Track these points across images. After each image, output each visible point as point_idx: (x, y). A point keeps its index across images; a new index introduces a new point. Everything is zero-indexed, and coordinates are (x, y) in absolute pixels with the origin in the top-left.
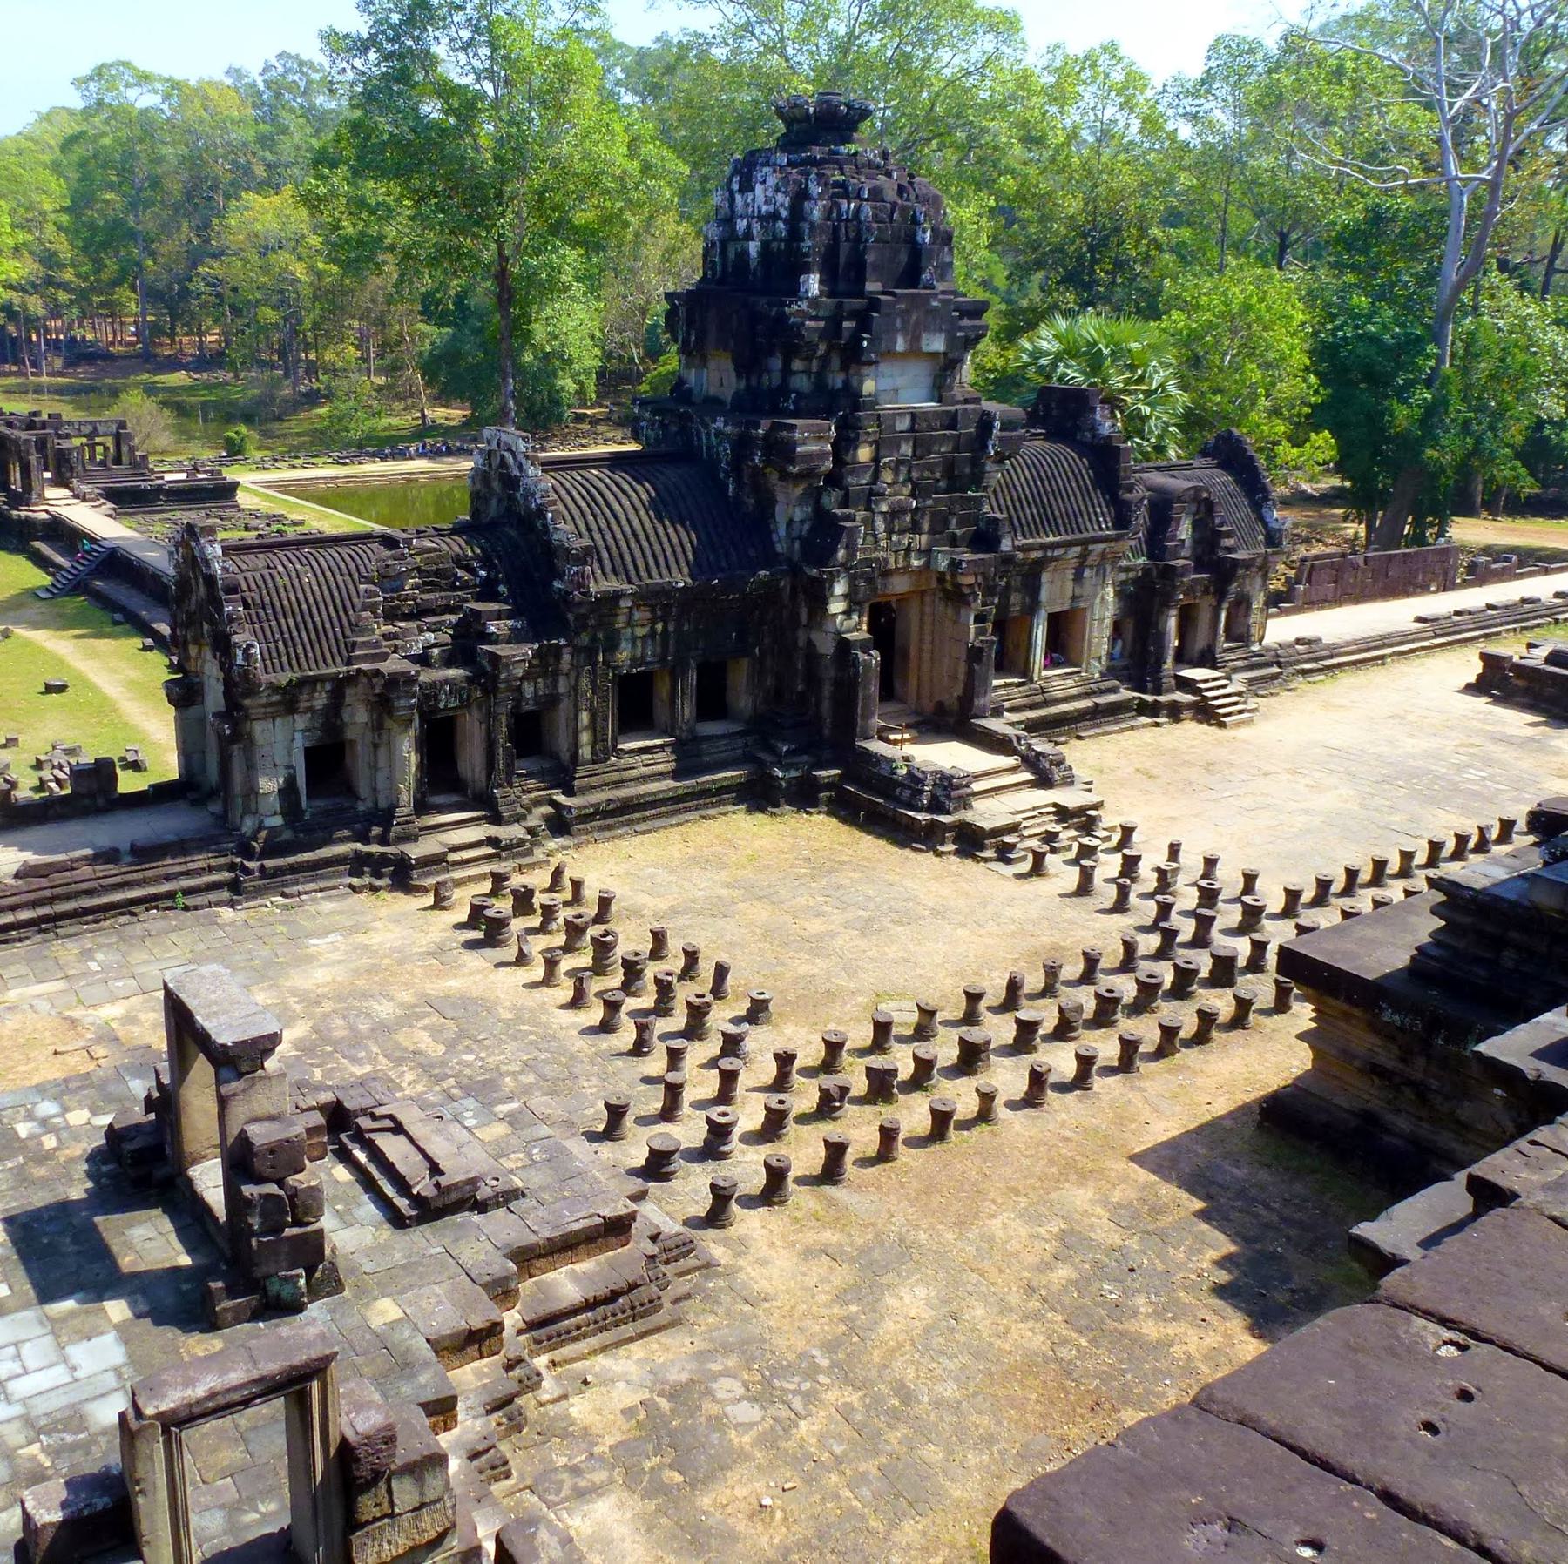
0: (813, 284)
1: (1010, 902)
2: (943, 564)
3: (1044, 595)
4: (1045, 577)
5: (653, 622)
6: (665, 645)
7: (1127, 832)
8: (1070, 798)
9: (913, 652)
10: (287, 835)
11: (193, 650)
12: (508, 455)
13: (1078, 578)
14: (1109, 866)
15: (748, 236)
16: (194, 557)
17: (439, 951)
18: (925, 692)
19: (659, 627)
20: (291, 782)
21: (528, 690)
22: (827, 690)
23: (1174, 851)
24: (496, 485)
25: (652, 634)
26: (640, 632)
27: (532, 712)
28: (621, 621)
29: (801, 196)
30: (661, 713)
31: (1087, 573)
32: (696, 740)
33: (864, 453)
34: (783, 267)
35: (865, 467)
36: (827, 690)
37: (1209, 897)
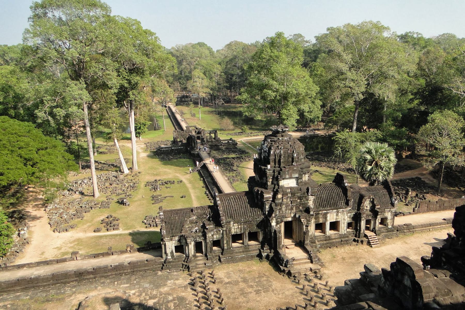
2: (297, 216)
3: (328, 218)
4: (328, 215)
5: (238, 225)
6: (241, 230)
9: (295, 230)
10: (171, 260)
19: (240, 226)
20: (172, 251)
21: (215, 236)
25: (238, 228)
26: (236, 227)
28: (231, 226)
31: (339, 214)
33: (280, 196)
35: (280, 199)
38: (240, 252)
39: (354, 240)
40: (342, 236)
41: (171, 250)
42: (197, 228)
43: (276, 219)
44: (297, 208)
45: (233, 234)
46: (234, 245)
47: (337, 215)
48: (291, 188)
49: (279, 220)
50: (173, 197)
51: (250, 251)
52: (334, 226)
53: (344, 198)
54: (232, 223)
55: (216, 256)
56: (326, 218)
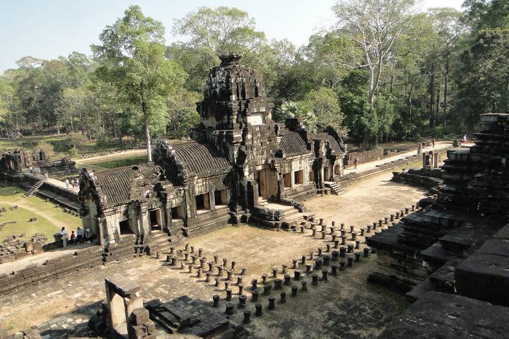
0: (234, 97)
1: (298, 240)
2: (270, 161)
3: (293, 168)
4: (293, 163)
7: (321, 220)
8: (307, 214)
9: (265, 184)
10: (117, 245)
11: (86, 201)
12: (163, 145)
13: (300, 163)
14: (319, 228)
15: (216, 87)
16: (86, 177)
17: (160, 269)
18: (268, 193)
21: (174, 201)
22: (246, 194)
23: (333, 224)
24: (160, 152)
25: (203, 185)
26: (200, 185)
27: (175, 208)
29: (228, 77)
30: (206, 204)
31: (302, 161)
32: (216, 210)
33: (249, 136)
34: (226, 94)
35: (249, 140)
36: (246, 194)
37: (343, 233)
38: (208, 220)
39: (318, 192)
40: (306, 189)
41: (114, 229)
42: (148, 191)
43: (249, 167)
44: (268, 152)
45: (197, 195)
46: (199, 212)
47: (300, 163)
48: (260, 127)
49: (251, 168)
50: (15, 222)
51: (218, 217)
52: (298, 175)
53: (303, 142)
54: (196, 178)
55: (178, 230)
56: (291, 167)
